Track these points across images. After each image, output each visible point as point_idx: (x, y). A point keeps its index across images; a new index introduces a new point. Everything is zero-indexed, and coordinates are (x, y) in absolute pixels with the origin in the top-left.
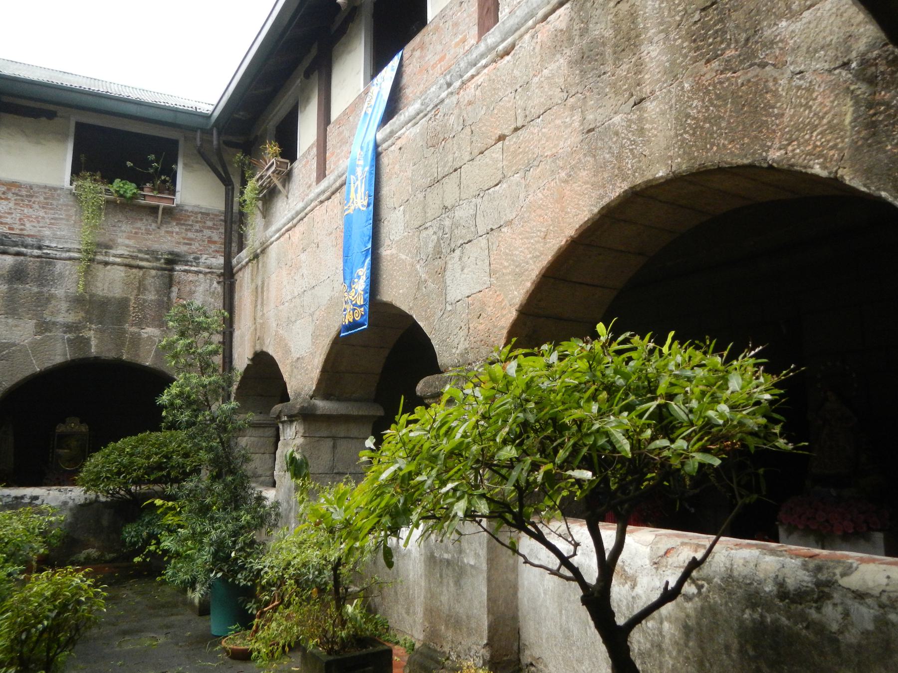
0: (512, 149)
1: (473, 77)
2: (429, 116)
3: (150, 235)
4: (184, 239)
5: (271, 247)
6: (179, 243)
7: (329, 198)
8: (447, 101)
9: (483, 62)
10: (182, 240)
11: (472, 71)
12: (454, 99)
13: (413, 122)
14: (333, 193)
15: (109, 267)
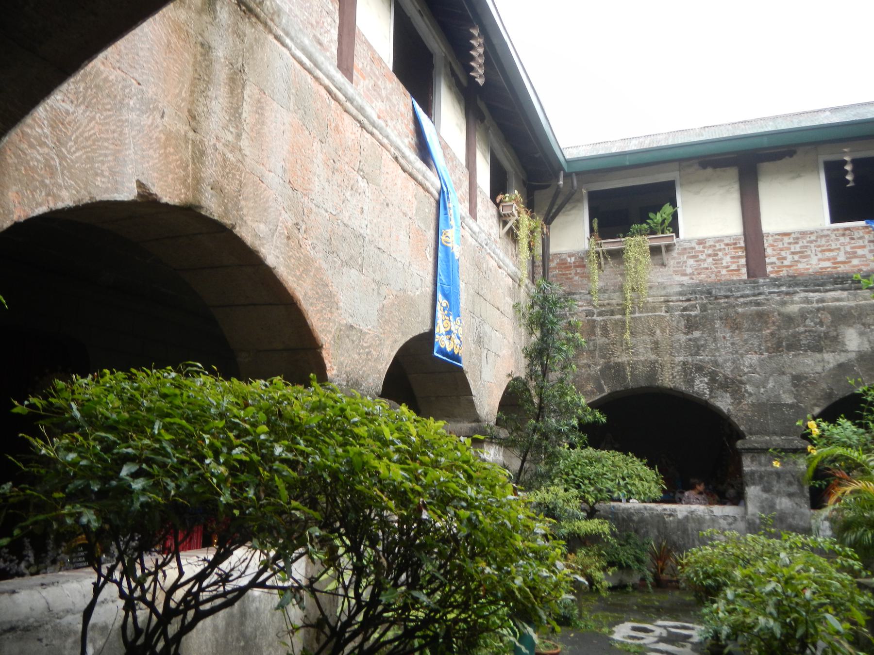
14: (410, 175)
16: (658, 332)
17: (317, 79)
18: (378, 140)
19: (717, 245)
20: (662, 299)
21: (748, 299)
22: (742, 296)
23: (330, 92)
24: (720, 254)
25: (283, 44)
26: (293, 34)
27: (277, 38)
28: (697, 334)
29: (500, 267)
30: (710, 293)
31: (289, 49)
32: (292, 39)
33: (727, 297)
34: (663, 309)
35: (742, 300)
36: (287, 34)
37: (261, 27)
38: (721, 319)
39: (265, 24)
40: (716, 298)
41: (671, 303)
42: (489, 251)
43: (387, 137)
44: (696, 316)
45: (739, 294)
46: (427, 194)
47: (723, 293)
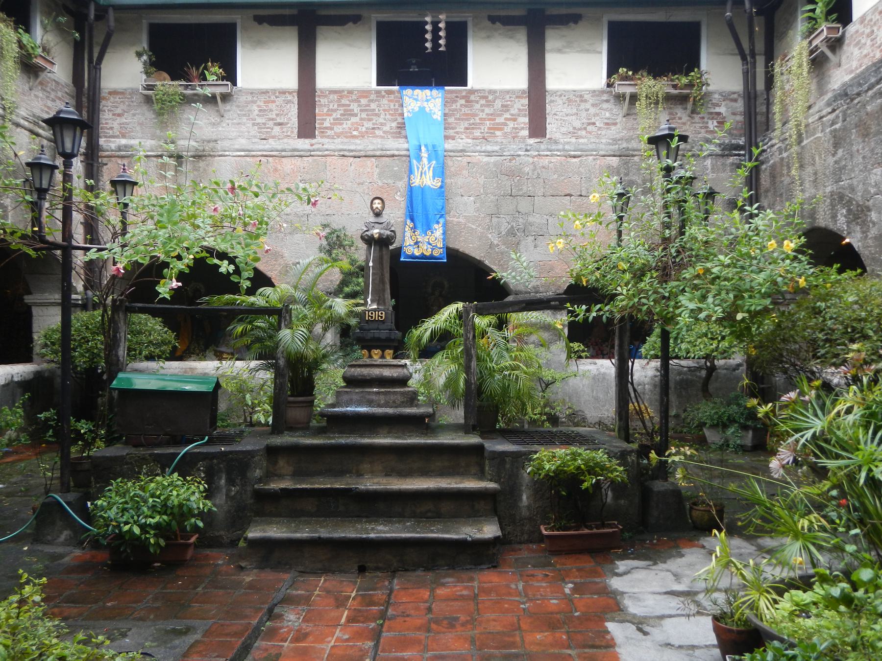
0: (577, 203)
1: (547, 156)
2: (505, 158)
3: (25, 95)
4: (45, 106)
5: (216, 158)
6: (42, 110)
7: (355, 157)
8: (522, 157)
9: (559, 153)
10: (43, 107)
11: (548, 153)
12: (531, 160)
13: (487, 154)
14: (365, 156)
15: (19, 130)
16: (817, 159)
17: (253, 156)
18: (319, 156)
19: (873, 17)
20: (817, 117)
21: (875, 90)
22: (869, 89)
23: (266, 156)
24: (875, 29)
25: (225, 156)
26: (227, 149)
27: (220, 156)
28: (840, 152)
29: (575, 157)
30: (846, 95)
31: (229, 156)
32: (228, 151)
33: (859, 94)
34: (820, 128)
35: (870, 93)
36: (225, 151)
37: (210, 158)
38: (856, 126)
39: (210, 156)
40: (852, 100)
41: (824, 119)
42: (537, 153)
43: (327, 150)
44: (840, 129)
45: (865, 87)
46: (396, 158)
47: (856, 90)
